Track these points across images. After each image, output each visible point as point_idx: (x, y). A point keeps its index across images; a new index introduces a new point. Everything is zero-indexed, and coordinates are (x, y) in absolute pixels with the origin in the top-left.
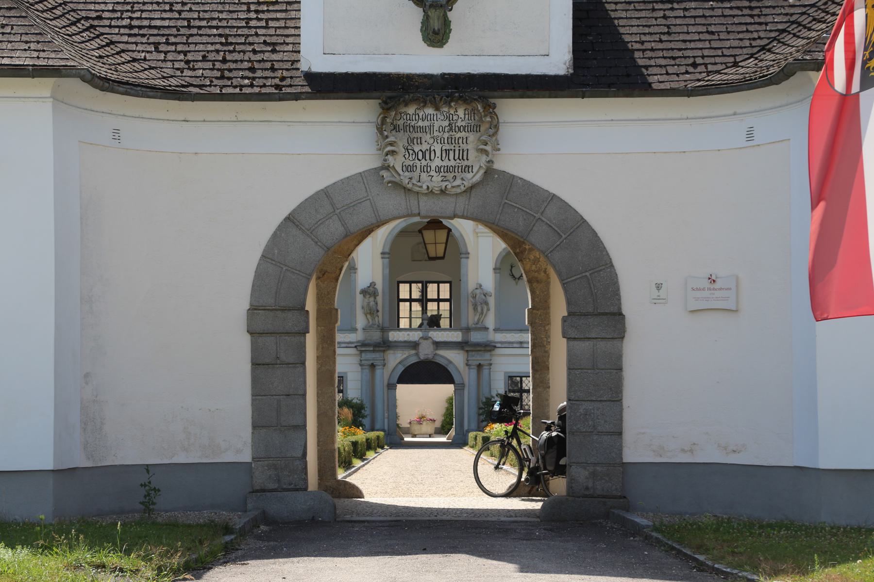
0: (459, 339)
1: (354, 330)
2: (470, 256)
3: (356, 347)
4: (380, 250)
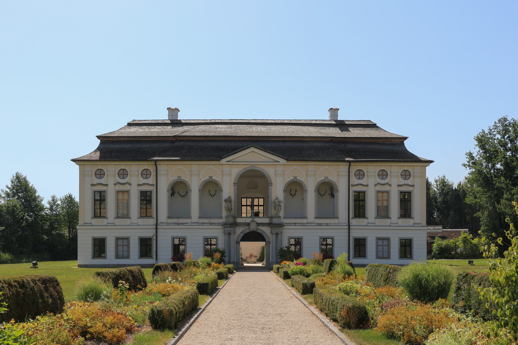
0: (268, 222)
1: (221, 217)
2: (273, 185)
3: (222, 225)
4: (233, 182)
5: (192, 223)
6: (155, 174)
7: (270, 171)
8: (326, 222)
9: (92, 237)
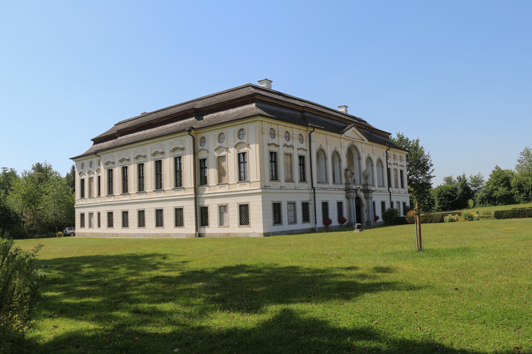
2: (362, 158)
3: (344, 190)
5: (330, 188)
6: (308, 139)
7: (359, 146)
8: (382, 190)
9: (238, 203)
